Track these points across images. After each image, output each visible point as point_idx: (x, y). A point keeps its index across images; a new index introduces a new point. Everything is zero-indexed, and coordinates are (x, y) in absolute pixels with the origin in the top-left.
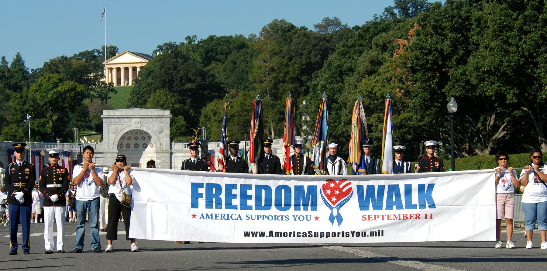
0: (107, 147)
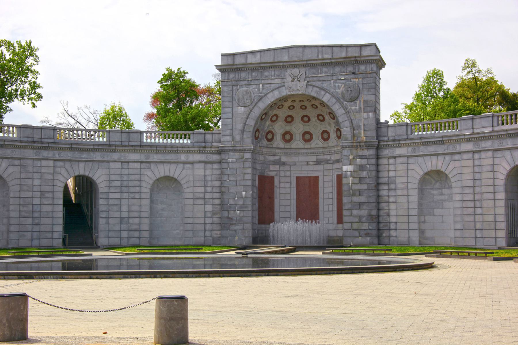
0: (228, 138)
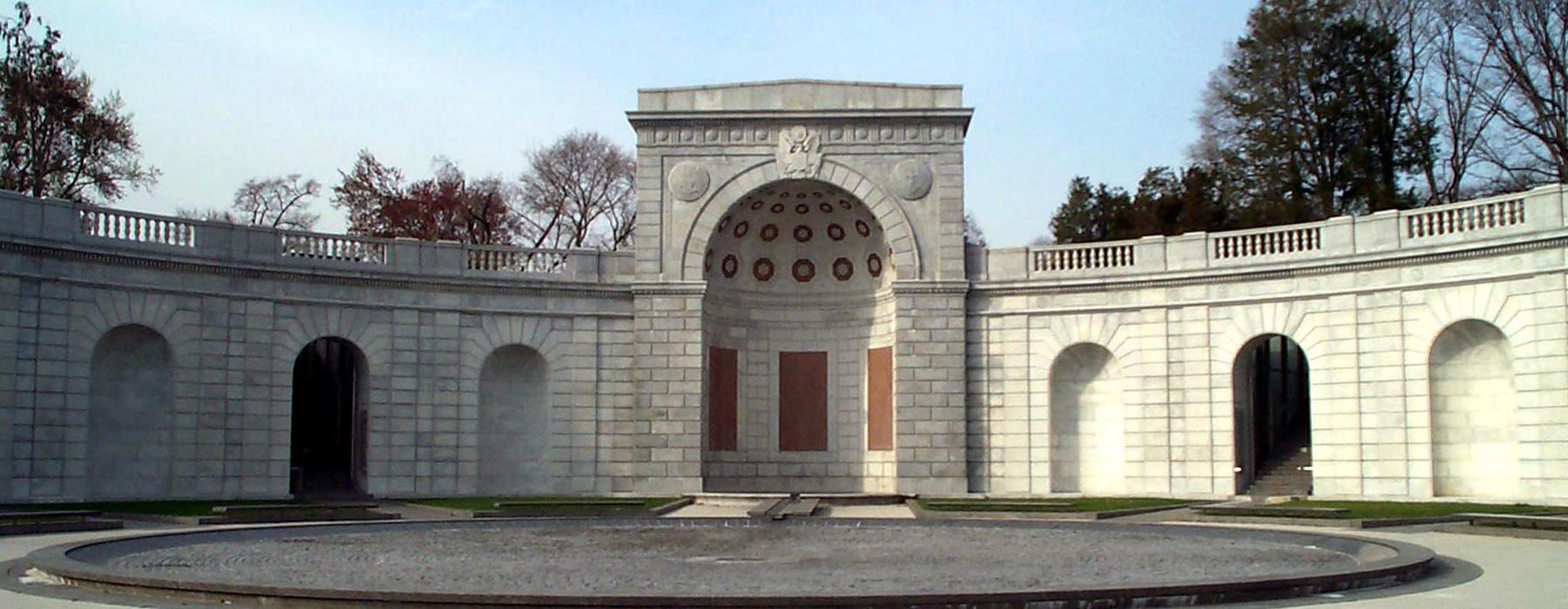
0: (653, 266)
